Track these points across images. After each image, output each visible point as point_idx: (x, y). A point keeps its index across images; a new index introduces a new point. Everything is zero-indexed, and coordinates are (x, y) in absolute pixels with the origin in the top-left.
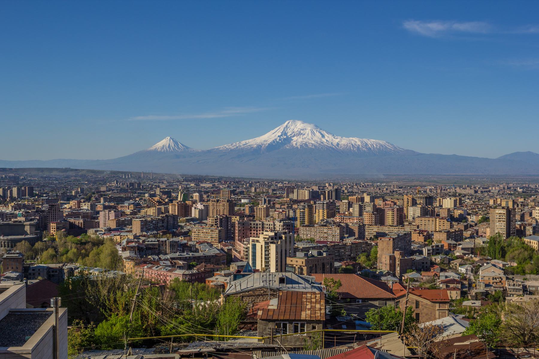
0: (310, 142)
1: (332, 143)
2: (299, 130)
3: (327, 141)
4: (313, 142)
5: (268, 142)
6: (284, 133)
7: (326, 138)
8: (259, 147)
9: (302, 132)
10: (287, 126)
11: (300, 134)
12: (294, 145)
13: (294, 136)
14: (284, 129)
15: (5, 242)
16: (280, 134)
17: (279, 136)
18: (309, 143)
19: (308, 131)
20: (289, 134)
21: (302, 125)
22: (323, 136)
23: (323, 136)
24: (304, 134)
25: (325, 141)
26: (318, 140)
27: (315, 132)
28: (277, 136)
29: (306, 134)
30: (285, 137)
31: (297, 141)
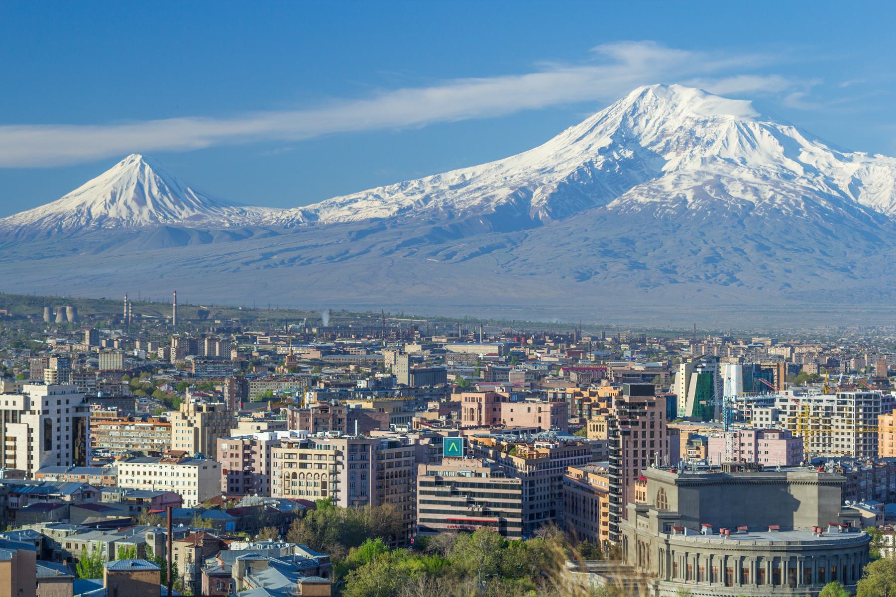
0: (735, 173)
1: (828, 181)
2: (689, 124)
3: (808, 168)
4: (748, 176)
5: (560, 177)
6: (624, 137)
7: (804, 157)
8: (521, 196)
9: (699, 131)
10: (635, 108)
11: (691, 139)
12: (669, 187)
13: (666, 150)
14: (625, 118)
15: (777, 560)
16: (606, 141)
17: (602, 151)
18: (731, 180)
19: (724, 128)
20: (644, 143)
21: (700, 102)
22: (792, 149)
23: (792, 149)
24: (710, 143)
25: (800, 171)
26: (772, 168)
27: (756, 132)
28: (595, 148)
29: (718, 144)
30: (629, 154)
31: (680, 177)
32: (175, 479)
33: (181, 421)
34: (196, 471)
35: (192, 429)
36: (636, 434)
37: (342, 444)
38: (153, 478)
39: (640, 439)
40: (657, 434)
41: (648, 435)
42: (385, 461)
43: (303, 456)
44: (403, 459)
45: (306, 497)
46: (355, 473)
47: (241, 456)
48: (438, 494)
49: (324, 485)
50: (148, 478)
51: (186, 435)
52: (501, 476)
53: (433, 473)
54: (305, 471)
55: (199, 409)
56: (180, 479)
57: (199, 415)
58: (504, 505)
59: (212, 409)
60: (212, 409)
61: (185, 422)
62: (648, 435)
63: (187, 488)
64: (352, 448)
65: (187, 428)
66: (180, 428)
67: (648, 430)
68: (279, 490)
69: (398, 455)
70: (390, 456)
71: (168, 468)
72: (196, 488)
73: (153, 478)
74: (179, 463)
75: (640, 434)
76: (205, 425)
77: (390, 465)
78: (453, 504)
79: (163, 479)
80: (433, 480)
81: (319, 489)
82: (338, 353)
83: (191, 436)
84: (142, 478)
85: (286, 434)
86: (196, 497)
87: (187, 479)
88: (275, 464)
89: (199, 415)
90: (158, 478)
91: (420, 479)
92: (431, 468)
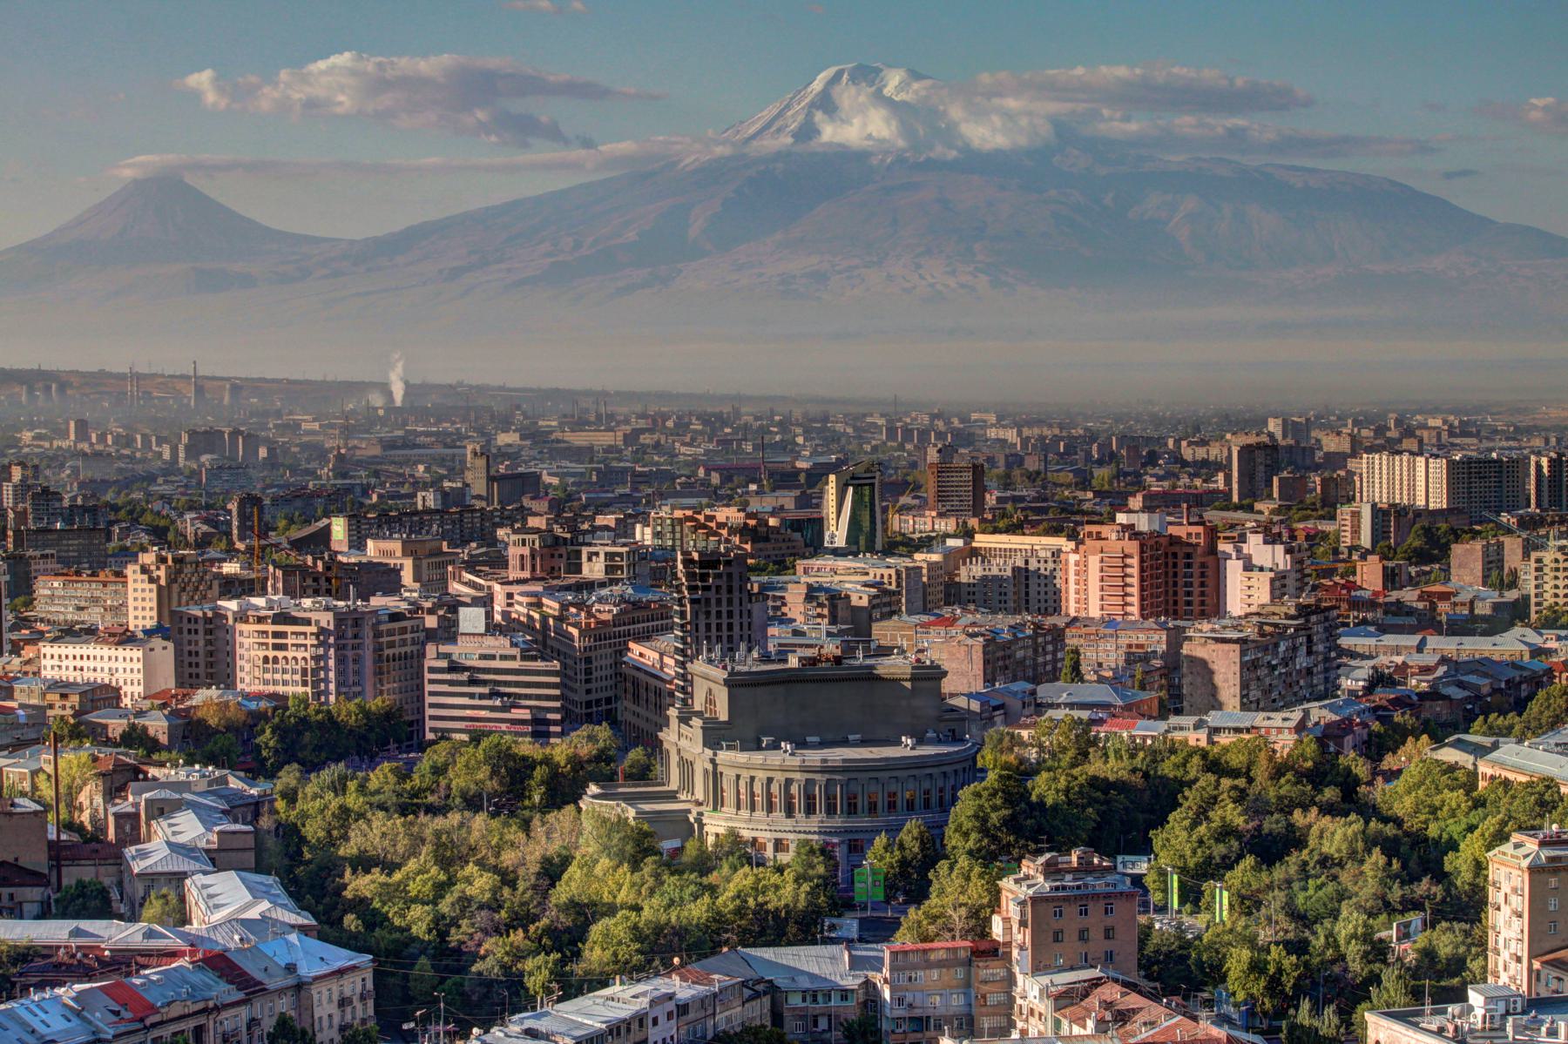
32: (113, 665)
33: (140, 577)
34: (140, 654)
35: (154, 586)
36: (708, 601)
37: (326, 620)
38: (85, 664)
39: (714, 610)
40: (736, 601)
41: (724, 603)
42: (385, 639)
43: (276, 635)
44: (408, 636)
45: (280, 689)
46: (345, 656)
47: (201, 632)
48: (451, 683)
49: (304, 672)
50: (79, 663)
51: (147, 595)
52: (534, 658)
53: (447, 656)
54: (280, 654)
55: (163, 560)
56: (120, 665)
57: (163, 567)
58: (538, 697)
59: (179, 561)
60: (179, 561)
61: (145, 577)
62: (724, 603)
63: (129, 676)
64: (340, 618)
65: (147, 586)
66: (140, 586)
67: (724, 596)
68: (247, 680)
69: (403, 631)
70: (391, 633)
71: (105, 651)
72: (141, 676)
73: (85, 664)
74: (119, 643)
75: (713, 601)
76: (171, 580)
77: (391, 645)
78: (472, 696)
79: (99, 665)
80: (444, 664)
81: (297, 677)
82: (405, 446)
83: (154, 595)
84: (71, 663)
85: (260, 601)
86: (141, 689)
87: (129, 666)
88: (242, 645)
89: (163, 567)
90: (92, 664)
91: (428, 663)
92: (443, 649)
